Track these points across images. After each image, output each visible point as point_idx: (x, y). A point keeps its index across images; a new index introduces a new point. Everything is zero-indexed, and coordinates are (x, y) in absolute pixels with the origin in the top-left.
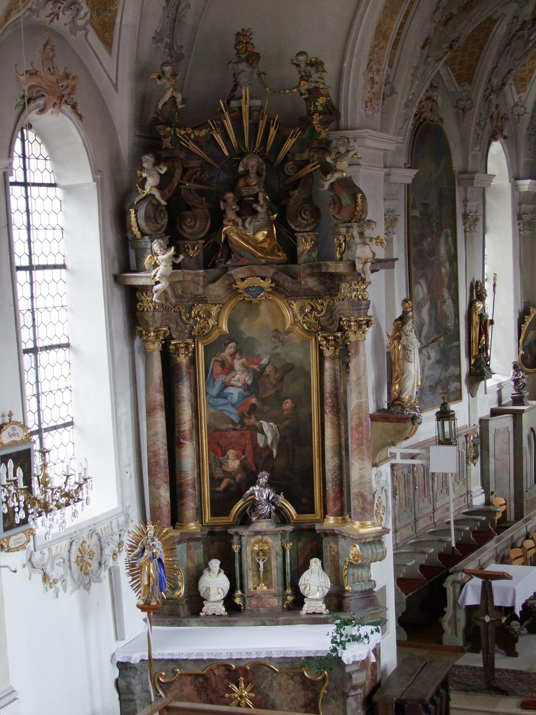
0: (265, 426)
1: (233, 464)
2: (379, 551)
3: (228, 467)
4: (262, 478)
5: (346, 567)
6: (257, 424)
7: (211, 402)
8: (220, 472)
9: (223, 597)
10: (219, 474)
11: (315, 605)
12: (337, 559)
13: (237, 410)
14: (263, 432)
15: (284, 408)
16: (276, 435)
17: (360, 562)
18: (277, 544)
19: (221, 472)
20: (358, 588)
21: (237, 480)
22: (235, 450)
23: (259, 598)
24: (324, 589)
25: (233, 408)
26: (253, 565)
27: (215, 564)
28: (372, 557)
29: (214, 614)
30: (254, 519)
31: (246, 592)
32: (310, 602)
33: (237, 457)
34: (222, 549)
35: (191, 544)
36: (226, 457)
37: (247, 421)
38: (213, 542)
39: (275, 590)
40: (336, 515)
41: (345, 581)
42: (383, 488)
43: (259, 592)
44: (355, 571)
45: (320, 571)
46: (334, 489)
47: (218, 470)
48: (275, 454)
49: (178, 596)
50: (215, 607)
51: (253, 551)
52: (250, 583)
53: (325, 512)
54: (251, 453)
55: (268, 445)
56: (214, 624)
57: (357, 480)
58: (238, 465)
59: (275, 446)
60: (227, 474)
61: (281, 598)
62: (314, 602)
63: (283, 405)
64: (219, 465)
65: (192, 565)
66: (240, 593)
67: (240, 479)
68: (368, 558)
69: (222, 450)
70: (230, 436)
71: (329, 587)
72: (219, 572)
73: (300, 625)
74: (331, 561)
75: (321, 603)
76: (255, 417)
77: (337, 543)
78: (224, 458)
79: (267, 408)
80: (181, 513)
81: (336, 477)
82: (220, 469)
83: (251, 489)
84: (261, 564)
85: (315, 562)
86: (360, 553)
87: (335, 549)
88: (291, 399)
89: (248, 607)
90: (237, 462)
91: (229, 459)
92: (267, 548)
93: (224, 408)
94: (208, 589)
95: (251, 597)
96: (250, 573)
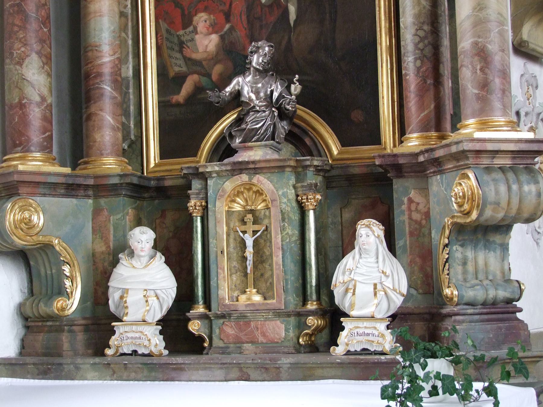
2: (526, 188)
3: (197, 51)
4: (256, 52)
5: (446, 241)
8: (178, 62)
9: (159, 316)
10: (177, 67)
11: (367, 331)
12: (425, 231)
17: (474, 215)
18: (285, 195)
19: (181, 62)
20: (476, 294)
21: (215, 77)
22: (210, 14)
23: (242, 318)
24: (391, 294)
26: (232, 245)
27: (143, 238)
28: (509, 203)
29: (135, 352)
30: (238, 141)
31: (214, 305)
33: (214, 28)
34: (168, 208)
35: (103, 202)
36: (191, 28)
38: (163, 215)
39: (279, 302)
40: (424, 128)
41: (444, 277)
42: (539, 114)
43: (241, 308)
44: (470, 254)
45: (381, 249)
46: (418, 69)
47: (177, 59)
48: (293, 16)
49: (63, 309)
50: (137, 335)
51: (229, 213)
52: (224, 288)
53: (402, 130)
54: (244, 17)
56: (133, 375)
57: (468, 17)
58: (217, 46)
60: (194, 65)
62: (366, 324)
64: (177, 48)
65: (104, 249)
66: (200, 309)
67: (221, 75)
68: (498, 204)
69: (183, 15)
71: (404, 291)
72: (153, 257)
73: (331, 381)
74: (411, 234)
75: (382, 327)
77: (425, 190)
80: (87, 137)
81: (422, 39)
82: (178, 55)
83: (234, 82)
84: (249, 241)
85: (368, 226)
86: (477, 191)
87: (421, 207)
89: (217, 342)
90: (215, 38)
92: (263, 205)
94: (126, 291)
95: (223, 316)
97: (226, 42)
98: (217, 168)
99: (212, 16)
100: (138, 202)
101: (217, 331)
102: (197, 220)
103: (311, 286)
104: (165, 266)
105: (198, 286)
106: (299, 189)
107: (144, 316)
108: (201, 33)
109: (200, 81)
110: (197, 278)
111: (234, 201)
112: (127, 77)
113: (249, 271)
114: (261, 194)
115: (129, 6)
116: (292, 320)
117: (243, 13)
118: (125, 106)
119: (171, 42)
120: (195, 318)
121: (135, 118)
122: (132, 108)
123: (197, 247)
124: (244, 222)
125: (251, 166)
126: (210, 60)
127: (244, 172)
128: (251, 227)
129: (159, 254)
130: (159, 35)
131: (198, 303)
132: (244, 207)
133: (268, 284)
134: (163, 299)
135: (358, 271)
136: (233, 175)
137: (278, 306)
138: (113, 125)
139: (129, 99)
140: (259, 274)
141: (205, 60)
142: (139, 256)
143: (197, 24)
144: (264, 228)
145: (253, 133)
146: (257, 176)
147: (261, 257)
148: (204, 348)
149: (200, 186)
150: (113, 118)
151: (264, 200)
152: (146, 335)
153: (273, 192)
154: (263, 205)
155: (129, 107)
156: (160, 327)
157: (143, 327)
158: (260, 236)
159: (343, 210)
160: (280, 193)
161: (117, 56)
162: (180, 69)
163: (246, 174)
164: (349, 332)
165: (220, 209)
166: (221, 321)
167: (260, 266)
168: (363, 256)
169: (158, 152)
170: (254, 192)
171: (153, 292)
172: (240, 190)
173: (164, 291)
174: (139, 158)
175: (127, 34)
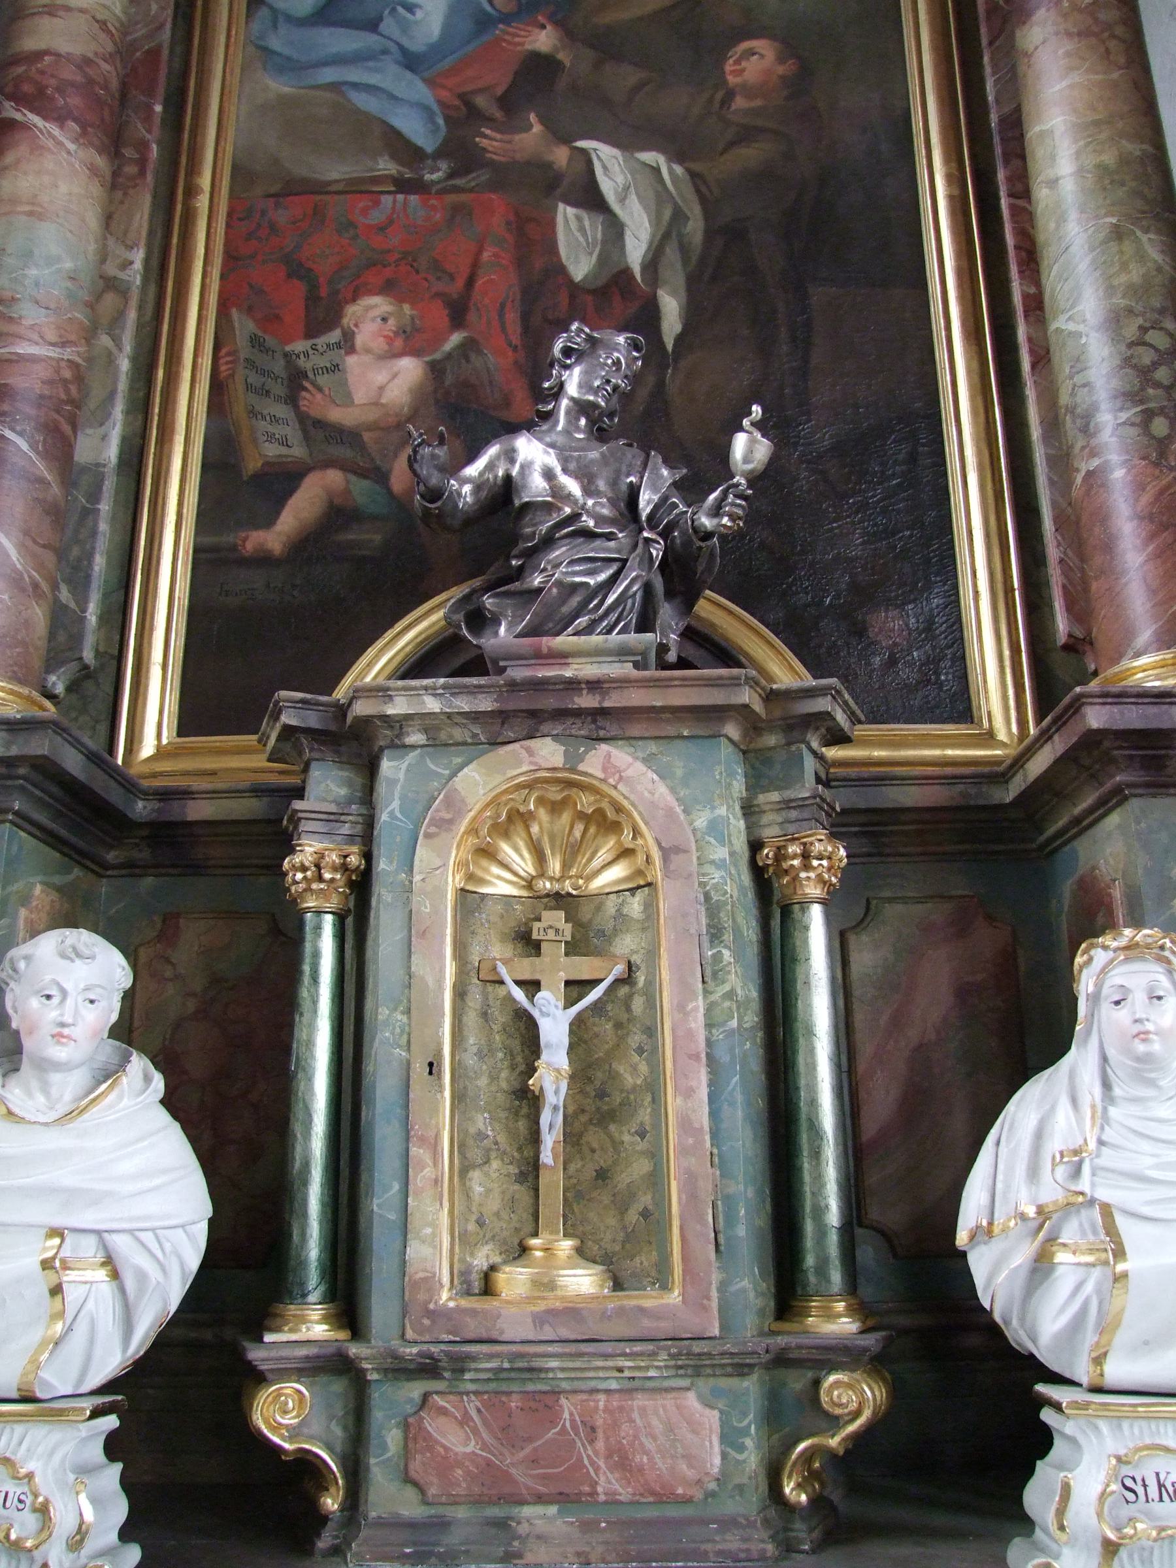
0: (611, 167)
1: (378, 373)
6: (560, 156)
7: (275, 43)
8: (279, 430)
9: (111, 1362)
10: (273, 440)
13: (430, 83)
14: (591, 198)
15: (732, 80)
16: (678, 216)
18: (714, 827)
19: (292, 432)
22: (400, 300)
23: (520, 1384)
25: (409, 75)
31: (381, 1311)
32: (1134, 1434)
33: (409, 341)
36: (335, 336)
37: (491, 142)
38: (168, 932)
39: (695, 1301)
47: (275, 420)
52: (430, 1234)
54: (512, 317)
55: (626, 272)
59: (674, 274)
60: (330, 440)
61: (751, 1386)
63: (729, 66)
64: (279, 389)
66: (313, 1326)
69: (312, 299)
70: (376, 217)
72: (109, 1074)
76: (542, 120)
78: (321, 341)
79: (623, 78)
82: (282, 411)
84: (554, 1024)
88: (773, 38)
89: (387, 1496)
90: (408, 372)
91: (352, 350)
92: (618, 871)
93: (354, 75)
95: (428, 1369)
96: (440, 1114)
97: (447, 383)
98: (432, 705)
99: (407, 308)
100: (77, 872)
101: (393, 1438)
102: (318, 928)
103: (821, 1230)
104: (163, 1117)
105: (305, 1215)
106: (766, 819)
107: (35, 1364)
108: (368, 351)
109: (347, 492)
110: (305, 1183)
111: (487, 853)
112: (98, 465)
113: (547, 1157)
114: (614, 827)
115: (138, 265)
116: (751, 1386)
117: (509, 304)
118: (75, 551)
119: (263, 373)
120: (284, 1374)
121: (106, 596)
122: (100, 562)
123: (310, 1044)
124: (528, 943)
125: (586, 701)
126: (387, 429)
127: (545, 728)
128: (555, 967)
129: (139, 1064)
130: (224, 351)
131: (304, 1296)
132: (529, 884)
133: (633, 1216)
134: (142, 1276)
135: (1108, 1158)
136: (495, 743)
137: (691, 1323)
138: (15, 570)
139: (94, 533)
140: (589, 1173)
141: (371, 427)
142: (45, 1066)
143: (356, 325)
144: (619, 969)
145: (575, 600)
146: (604, 747)
147: (599, 1100)
148: (323, 1519)
149: (343, 791)
150: (21, 547)
151: (626, 853)
152: (30, 1476)
153: (670, 813)
154: (618, 871)
155: (90, 556)
156: (111, 1422)
157: (19, 1429)
158: (597, 1006)
159: (852, 939)
160: (701, 822)
161: (68, 353)
162: (284, 450)
163: (556, 738)
164: (1114, 1475)
165: (431, 877)
166: (415, 1390)
167: (593, 1137)
168: (1117, 1091)
169: (175, 708)
170: (582, 816)
171: (91, 1242)
172: (522, 809)
173: (148, 1237)
174: (103, 729)
175: (117, 341)
